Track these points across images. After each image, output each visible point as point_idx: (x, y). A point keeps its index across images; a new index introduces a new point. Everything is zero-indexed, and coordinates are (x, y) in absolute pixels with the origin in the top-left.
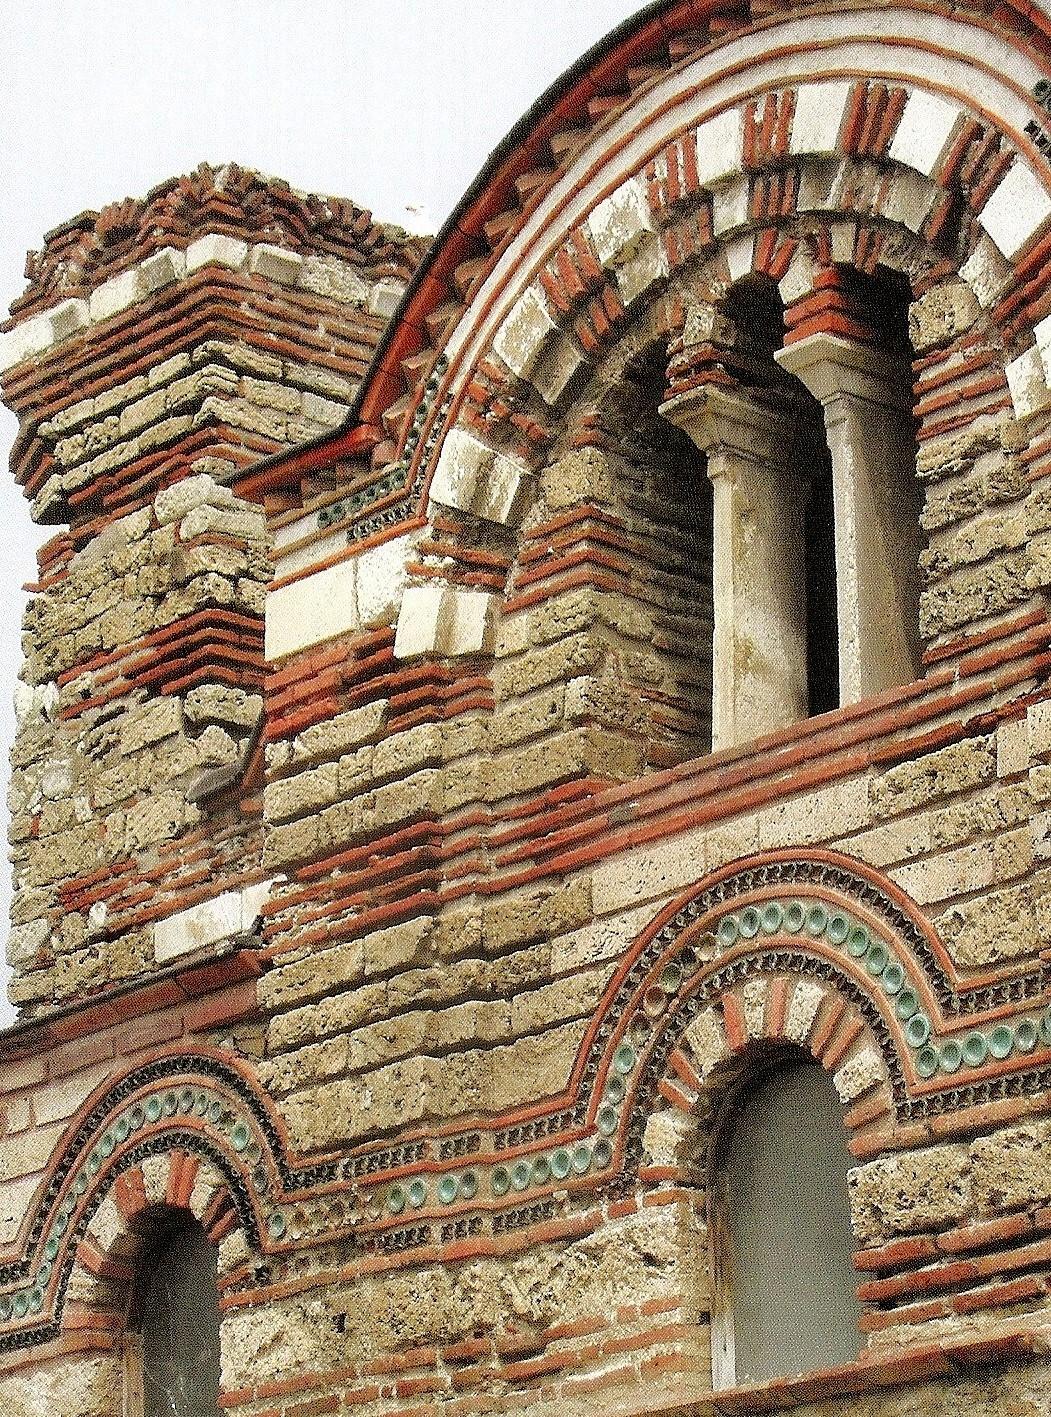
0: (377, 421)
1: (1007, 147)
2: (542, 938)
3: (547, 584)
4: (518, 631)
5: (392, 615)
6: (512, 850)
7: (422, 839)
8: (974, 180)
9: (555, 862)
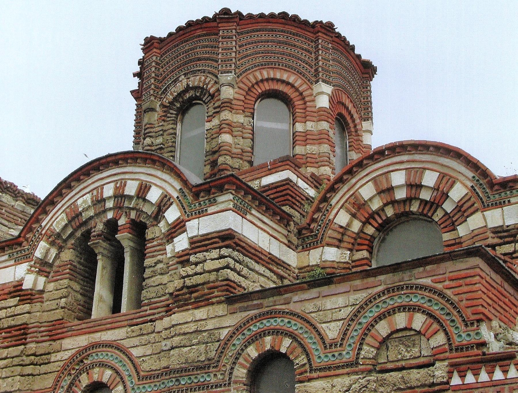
0: (24, 237)
1: (172, 200)
2: (49, 353)
3: (58, 277)
4: (51, 286)
5: (23, 279)
6: (44, 334)
7: (24, 329)
8: (164, 206)
9: (54, 337)
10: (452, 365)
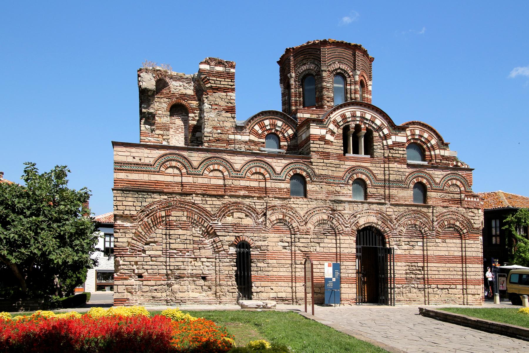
4: (336, 141)
10: (465, 195)
